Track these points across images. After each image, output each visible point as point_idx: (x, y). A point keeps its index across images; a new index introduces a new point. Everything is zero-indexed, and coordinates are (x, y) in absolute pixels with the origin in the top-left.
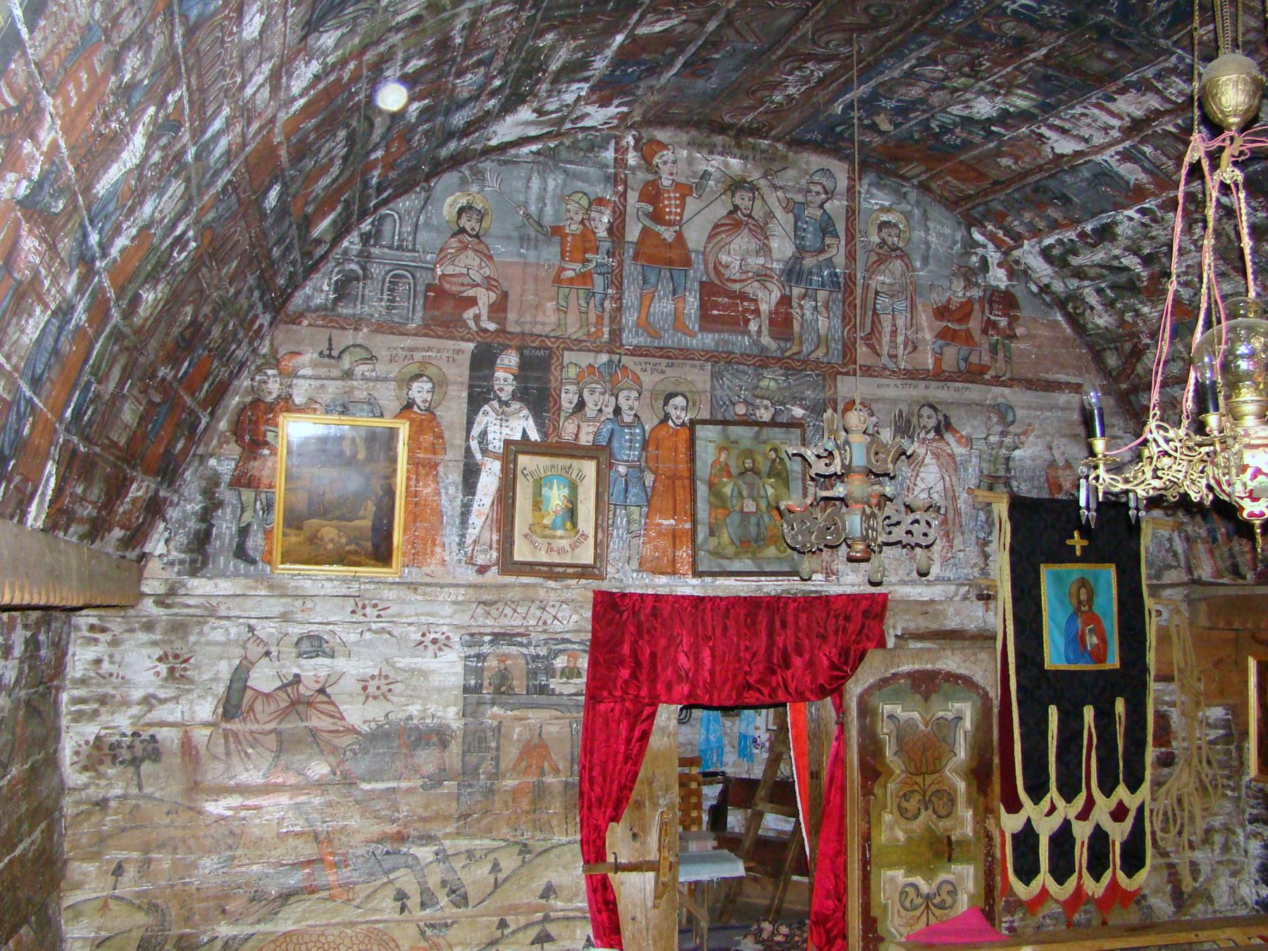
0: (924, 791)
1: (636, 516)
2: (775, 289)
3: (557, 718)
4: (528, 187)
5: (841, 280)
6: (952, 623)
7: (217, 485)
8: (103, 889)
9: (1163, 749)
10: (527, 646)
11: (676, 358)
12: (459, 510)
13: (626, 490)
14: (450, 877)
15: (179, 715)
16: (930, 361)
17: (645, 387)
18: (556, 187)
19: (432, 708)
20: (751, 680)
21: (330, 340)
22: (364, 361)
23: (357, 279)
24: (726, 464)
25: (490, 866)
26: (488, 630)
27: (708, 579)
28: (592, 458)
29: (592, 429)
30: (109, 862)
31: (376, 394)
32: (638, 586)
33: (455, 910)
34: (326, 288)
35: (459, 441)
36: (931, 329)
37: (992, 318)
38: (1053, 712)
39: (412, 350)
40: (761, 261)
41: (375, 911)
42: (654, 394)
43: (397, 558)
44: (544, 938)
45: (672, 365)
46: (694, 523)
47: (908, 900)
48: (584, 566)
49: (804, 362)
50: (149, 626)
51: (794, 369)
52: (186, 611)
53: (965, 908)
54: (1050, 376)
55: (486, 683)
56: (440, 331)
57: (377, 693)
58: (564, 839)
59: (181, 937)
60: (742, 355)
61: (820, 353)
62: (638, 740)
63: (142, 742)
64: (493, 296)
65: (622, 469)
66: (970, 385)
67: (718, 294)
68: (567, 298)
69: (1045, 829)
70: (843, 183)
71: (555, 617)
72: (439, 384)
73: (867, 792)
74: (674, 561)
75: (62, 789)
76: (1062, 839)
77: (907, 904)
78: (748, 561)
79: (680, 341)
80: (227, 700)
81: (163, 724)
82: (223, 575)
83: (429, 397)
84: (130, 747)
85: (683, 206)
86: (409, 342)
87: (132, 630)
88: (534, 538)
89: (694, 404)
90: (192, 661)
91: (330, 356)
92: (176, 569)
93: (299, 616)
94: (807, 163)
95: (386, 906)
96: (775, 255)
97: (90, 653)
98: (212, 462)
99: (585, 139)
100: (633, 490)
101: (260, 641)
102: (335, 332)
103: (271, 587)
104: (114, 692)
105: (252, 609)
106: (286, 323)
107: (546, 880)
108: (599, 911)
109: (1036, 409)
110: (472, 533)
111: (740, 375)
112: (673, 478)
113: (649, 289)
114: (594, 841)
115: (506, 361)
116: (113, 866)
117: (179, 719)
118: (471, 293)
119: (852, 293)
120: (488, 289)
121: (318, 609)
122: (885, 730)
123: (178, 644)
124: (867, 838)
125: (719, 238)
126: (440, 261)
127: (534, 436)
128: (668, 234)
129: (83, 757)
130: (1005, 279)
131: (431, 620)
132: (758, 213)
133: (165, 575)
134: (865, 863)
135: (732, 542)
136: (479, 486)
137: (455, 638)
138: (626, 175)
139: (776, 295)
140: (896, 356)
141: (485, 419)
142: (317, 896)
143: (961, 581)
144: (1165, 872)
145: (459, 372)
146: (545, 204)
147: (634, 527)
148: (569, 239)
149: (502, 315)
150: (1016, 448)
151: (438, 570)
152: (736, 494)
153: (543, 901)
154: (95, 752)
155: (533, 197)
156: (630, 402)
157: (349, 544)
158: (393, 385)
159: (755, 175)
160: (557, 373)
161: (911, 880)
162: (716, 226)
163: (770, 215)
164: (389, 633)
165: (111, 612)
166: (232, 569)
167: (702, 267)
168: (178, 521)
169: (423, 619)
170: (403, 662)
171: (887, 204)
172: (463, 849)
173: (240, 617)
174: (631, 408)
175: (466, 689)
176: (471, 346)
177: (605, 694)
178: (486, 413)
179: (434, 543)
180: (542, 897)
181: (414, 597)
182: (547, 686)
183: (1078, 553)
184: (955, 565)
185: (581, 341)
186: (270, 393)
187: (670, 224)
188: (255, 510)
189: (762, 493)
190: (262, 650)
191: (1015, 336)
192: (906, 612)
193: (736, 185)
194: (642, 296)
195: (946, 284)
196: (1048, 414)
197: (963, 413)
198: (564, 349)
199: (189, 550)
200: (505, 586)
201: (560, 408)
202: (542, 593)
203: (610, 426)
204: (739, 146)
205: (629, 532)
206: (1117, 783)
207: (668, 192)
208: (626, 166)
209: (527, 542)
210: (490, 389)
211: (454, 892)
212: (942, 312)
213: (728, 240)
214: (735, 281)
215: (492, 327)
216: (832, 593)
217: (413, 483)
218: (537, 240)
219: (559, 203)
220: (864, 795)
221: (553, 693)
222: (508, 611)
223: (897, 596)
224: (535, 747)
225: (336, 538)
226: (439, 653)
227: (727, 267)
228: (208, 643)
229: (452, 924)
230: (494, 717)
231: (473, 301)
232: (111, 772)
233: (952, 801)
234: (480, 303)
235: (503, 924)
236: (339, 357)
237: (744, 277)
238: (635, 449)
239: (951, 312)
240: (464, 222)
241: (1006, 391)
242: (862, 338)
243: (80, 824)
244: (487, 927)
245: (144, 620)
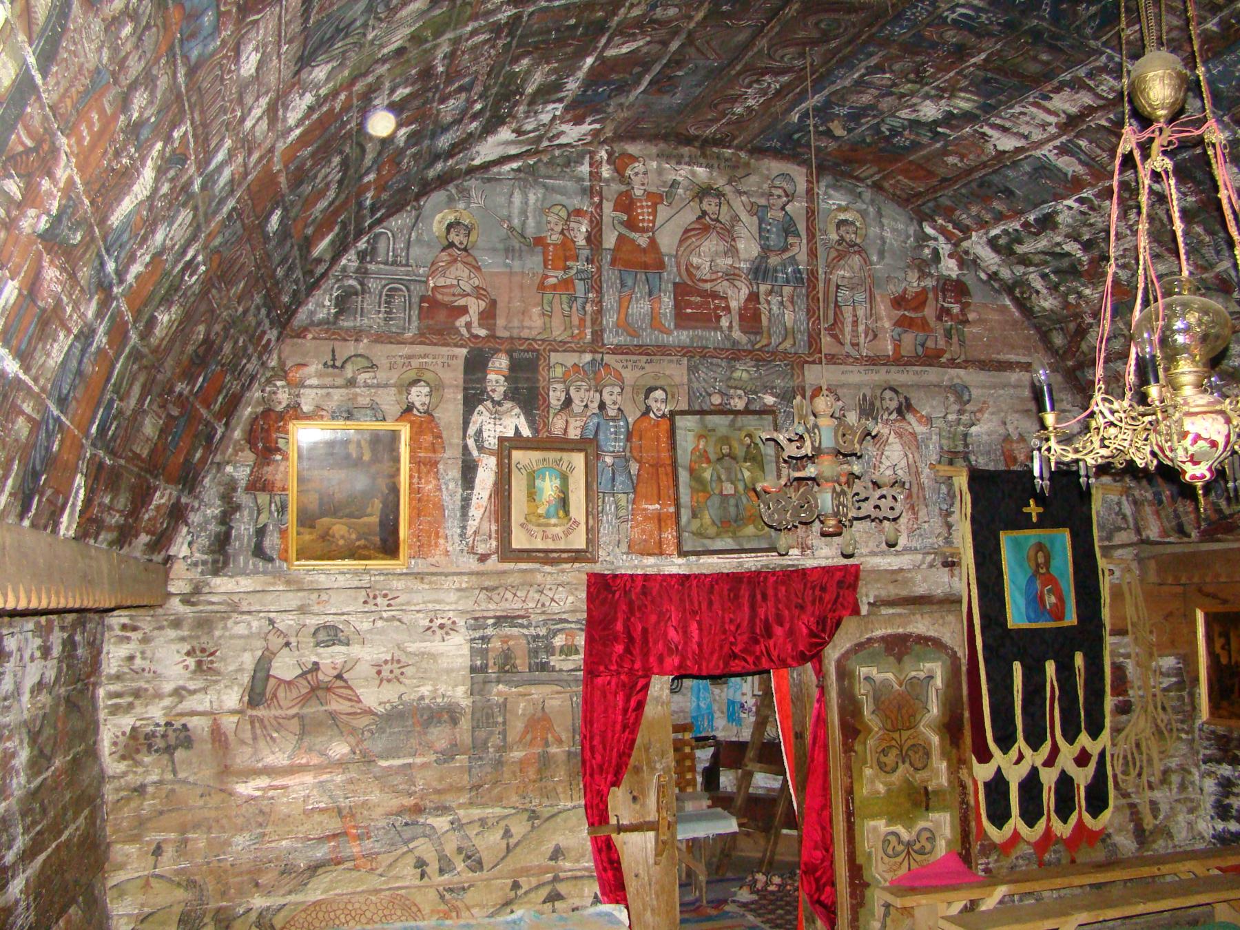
0: (901, 746)
1: (623, 503)
3: (558, 693)
4: (510, 202)
5: (804, 276)
6: (921, 590)
7: (234, 489)
8: (145, 869)
9: (1121, 698)
10: (527, 627)
11: (655, 355)
12: (459, 503)
13: (613, 479)
14: (465, 844)
15: (208, 704)
16: (890, 347)
18: (537, 200)
19: (442, 688)
20: (736, 650)
21: (333, 351)
22: (366, 369)
23: (356, 294)
25: (501, 832)
26: (491, 614)
27: (693, 558)
28: (580, 450)
29: (579, 424)
30: (148, 843)
31: (377, 400)
32: (628, 567)
33: (471, 874)
34: (327, 303)
35: (457, 440)
36: (889, 318)
38: (1017, 667)
39: (409, 357)
40: (730, 261)
41: (397, 878)
42: (635, 388)
43: (404, 550)
44: (555, 897)
45: (651, 361)
46: (678, 506)
48: (577, 551)
49: (773, 353)
50: (177, 623)
52: (210, 608)
53: (943, 853)
54: (1002, 357)
55: (491, 663)
56: (435, 338)
57: (391, 676)
58: (569, 804)
59: (219, 910)
62: (634, 710)
63: (175, 730)
64: (483, 304)
65: (609, 460)
66: (927, 368)
67: (690, 294)
68: (551, 303)
69: (1015, 776)
70: (802, 186)
71: (552, 600)
72: (436, 388)
73: (848, 749)
74: (660, 543)
75: (102, 778)
76: (1031, 784)
77: (890, 851)
78: (730, 540)
79: (657, 338)
80: (252, 689)
81: (193, 713)
82: (243, 573)
83: (427, 400)
84: (164, 736)
85: (654, 213)
86: (406, 350)
87: (161, 628)
88: (530, 526)
89: (673, 397)
90: (218, 654)
91: (334, 366)
92: (199, 570)
93: (316, 608)
94: (768, 169)
95: (408, 872)
96: (742, 256)
97: (123, 651)
98: (229, 469)
101: (280, 633)
102: (337, 344)
103: (288, 582)
104: (146, 686)
105: (272, 604)
106: (292, 337)
107: (554, 843)
108: (605, 869)
109: (989, 388)
110: (472, 525)
111: (714, 368)
112: (656, 466)
113: (626, 292)
114: (598, 805)
115: (497, 364)
116: (153, 847)
117: (208, 709)
118: (462, 302)
119: (814, 287)
120: (477, 298)
121: (332, 601)
122: (862, 691)
123: (204, 639)
124: (850, 792)
125: (689, 241)
126: (432, 274)
127: (526, 432)
128: (642, 240)
129: (121, 746)
130: (956, 268)
131: (438, 607)
132: (725, 217)
133: (190, 575)
134: (849, 815)
135: (714, 523)
136: (477, 481)
137: (461, 623)
138: (601, 187)
139: (745, 292)
140: (858, 344)
141: (480, 419)
142: (342, 867)
144: (1128, 812)
145: (454, 376)
146: (527, 218)
147: (622, 513)
148: (551, 248)
149: (491, 322)
150: (973, 424)
151: (443, 560)
152: (715, 478)
153: (553, 863)
154: (131, 742)
156: (614, 397)
157: (358, 539)
158: (393, 390)
159: (720, 182)
160: (544, 373)
161: (892, 829)
162: (686, 231)
163: (736, 218)
164: (400, 620)
165: (141, 612)
166: (251, 567)
167: (675, 269)
168: (199, 525)
169: (430, 606)
170: (413, 647)
171: (843, 203)
172: (476, 818)
173: (260, 612)
174: (615, 403)
175: (473, 669)
176: (464, 351)
177: (602, 668)
178: (480, 413)
179: (437, 536)
180: (551, 859)
181: (421, 586)
182: (548, 663)
183: (1034, 520)
184: (921, 535)
185: (565, 343)
186: (280, 403)
187: (643, 230)
188: (270, 512)
189: (739, 476)
190: (282, 641)
191: (967, 321)
192: (877, 581)
193: (703, 192)
194: (620, 298)
195: (901, 275)
196: (1001, 392)
197: (922, 394)
198: (550, 351)
199: (210, 551)
200: (504, 572)
201: (548, 406)
202: (539, 577)
203: (596, 420)
204: (704, 155)
205: (618, 518)
206: (1079, 732)
207: (641, 201)
208: (600, 179)
209: (524, 531)
210: (484, 391)
211: (469, 857)
212: (899, 302)
213: (697, 244)
214: (706, 281)
215: (483, 333)
217: (415, 480)
220: (845, 752)
221: (553, 669)
222: (509, 595)
223: (869, 567)
224: (539, 720)
225: (347, 535)
226: (446, 638)
227: (698, 268)
228: (232, 637)
229: (469, 887)
230: (499, 694)
231: (464, 310)
232: (147, 759)
233: (927, 754)
234: (471, 311)
235: (516, 886)
236: (342, 366)
237: (714, 277)
238: (620, 440)
240: (453, 237)
241: (962, 372)
243: (121, 809)
244: (502, 889)
245: (172, 617)
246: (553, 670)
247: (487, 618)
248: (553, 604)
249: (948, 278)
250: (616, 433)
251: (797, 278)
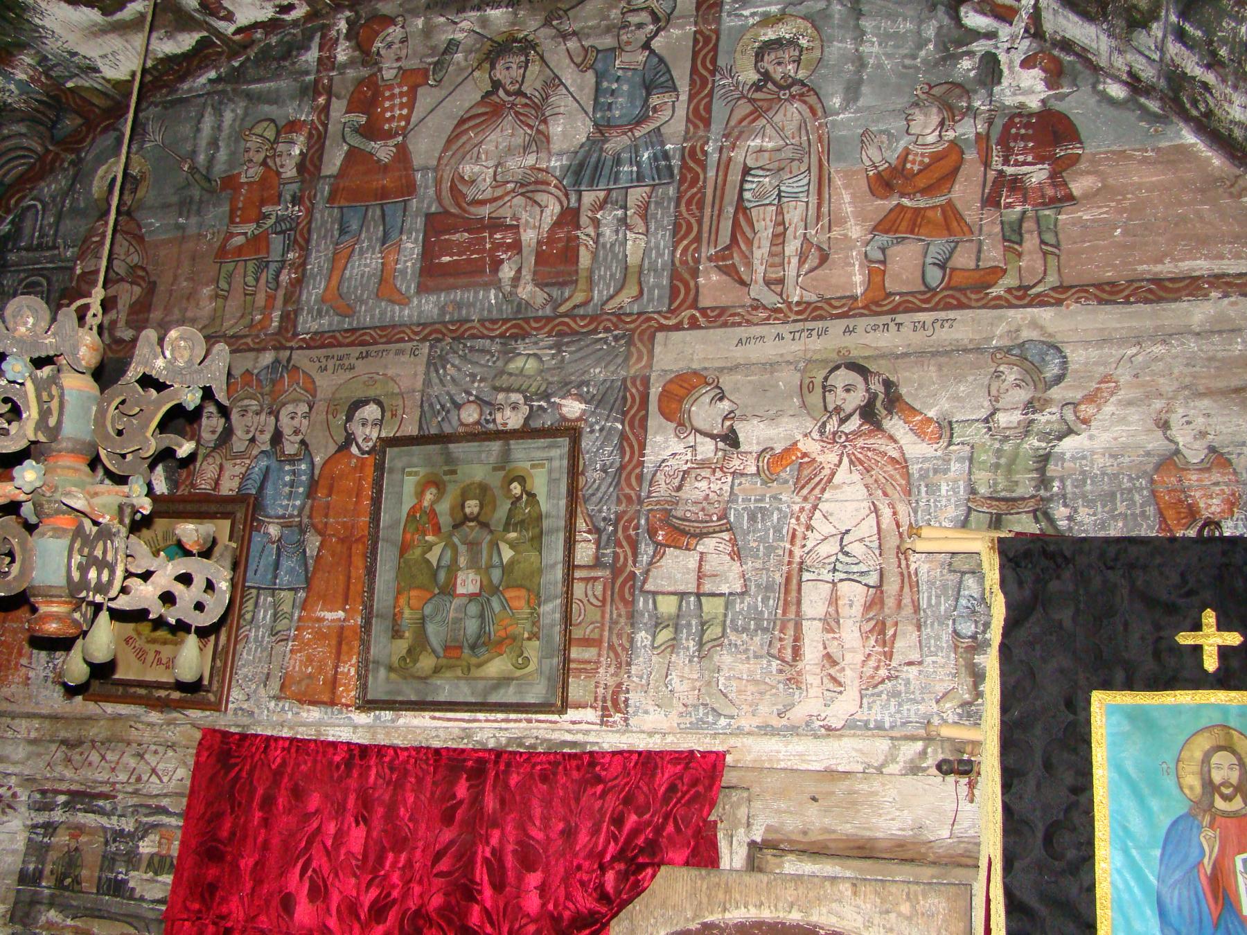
2: (552, 200)
4: (198, 130)
5: (676, 162)
10: (108, 815)
11: (375, 343)
13: (277, 565)
17: (320, 395)
24: (433, 511)
26: (64, 787)
27: (387, 715)
29: (239, 470)
36: (861, 216)
37: (1010, 170)
40: (530, 160)
42: (332, 406)
49: (594, 318)
51: (577, 333)
54: (1166, 268)
60: (482, 321)
61: (625, 298)
64: (137, 290)
65: (274, 530)
66: (951, 314)
71: (154, 771)
74: (334, 683)
79: (383, 313)
85: (411, 106)
96: (555, 147)
99: (280, 43)
100: (286, 564)
109: (1123, 342)
111: (475, 357)
112: (347, 541)
113: (348, 240)
119: (695, 180)
125: (464, 138)
128: (383, 151)
130: (1040, 86)
132: (533, 81)
138: (331, 79)
139: (553, 209)
140: (781, 281)
143: (909, 730)
146: (217, 148)
147: (282, 625)
150: (1070, 432)
155: (203, 142)
156: (296, 422)
162: (462, 121)
163: (554, 82)
167: (431, 191)
174: (296, 432)
175: (23, 877)
182: (125, 882)
183: (1211, 663)
184: (895, 694)
187: (390, 135)
191: (1070, 198)
192: (781, 794)
194: (335, 254)
195: (898, 124)
196: (1159, 349)
200: (90, 718)
203: (264, 463)
205: (273, 633)
207: (391, 88)
212: (884, 182)
213: (480, 138)
214: (482, 203)
216: (606, 747)
218: (201, 202)
219: (237, 141)
223: (748, 759)
237: (499, 192)
238: (297, 497)
239: (910, 177)
241: (1045, 315)
242: (710, 259)
246: (131, 898)
247: (58, 792)
248: (154, 779)
249: (1020, 112)
250: (292, 484)
251: (662, 169)
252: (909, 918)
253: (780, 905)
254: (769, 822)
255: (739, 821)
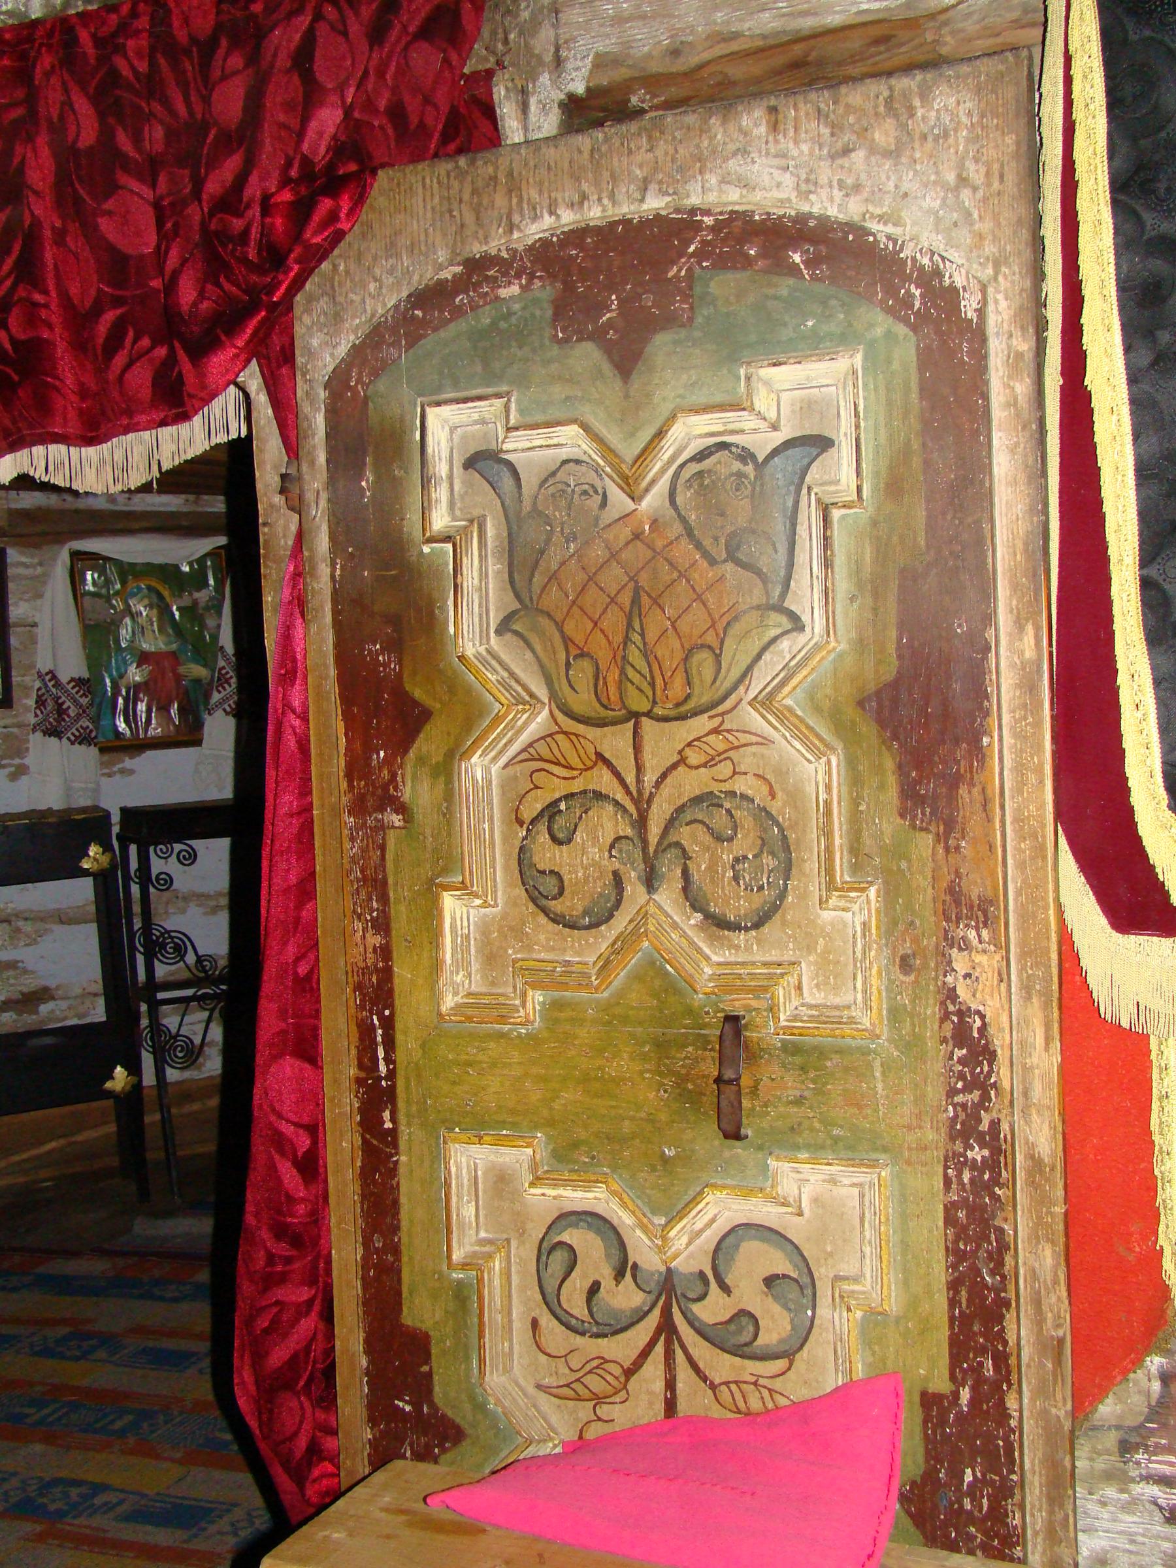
0: (643, 803)
47: (578, 1284)
53: (831, 1381)
77: (574, 1300)
161: (576, 1197)
220: (359, 807)
252: (893, 154)
253: (620, 196)
254: (601, 46)
255: (539, 58)
